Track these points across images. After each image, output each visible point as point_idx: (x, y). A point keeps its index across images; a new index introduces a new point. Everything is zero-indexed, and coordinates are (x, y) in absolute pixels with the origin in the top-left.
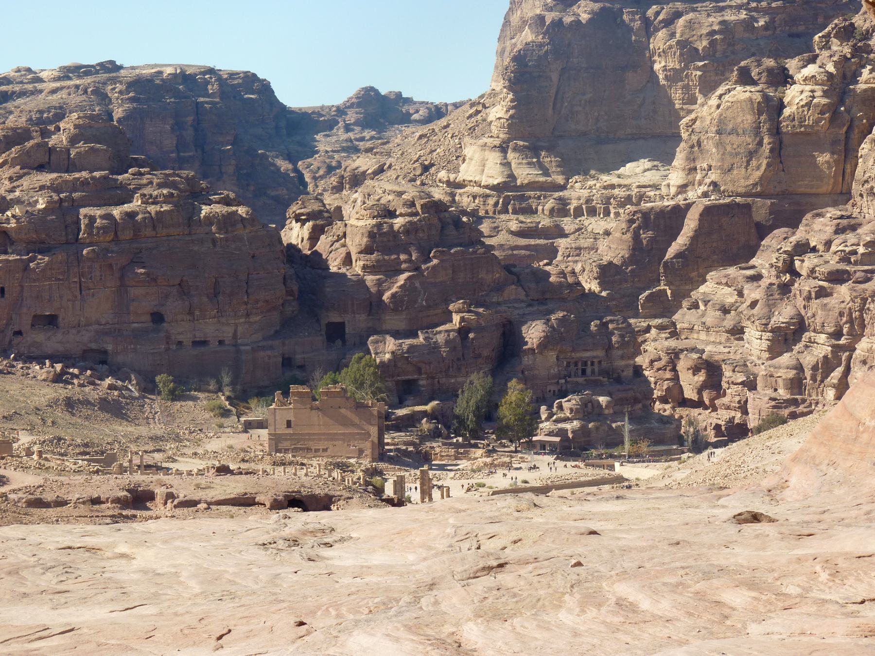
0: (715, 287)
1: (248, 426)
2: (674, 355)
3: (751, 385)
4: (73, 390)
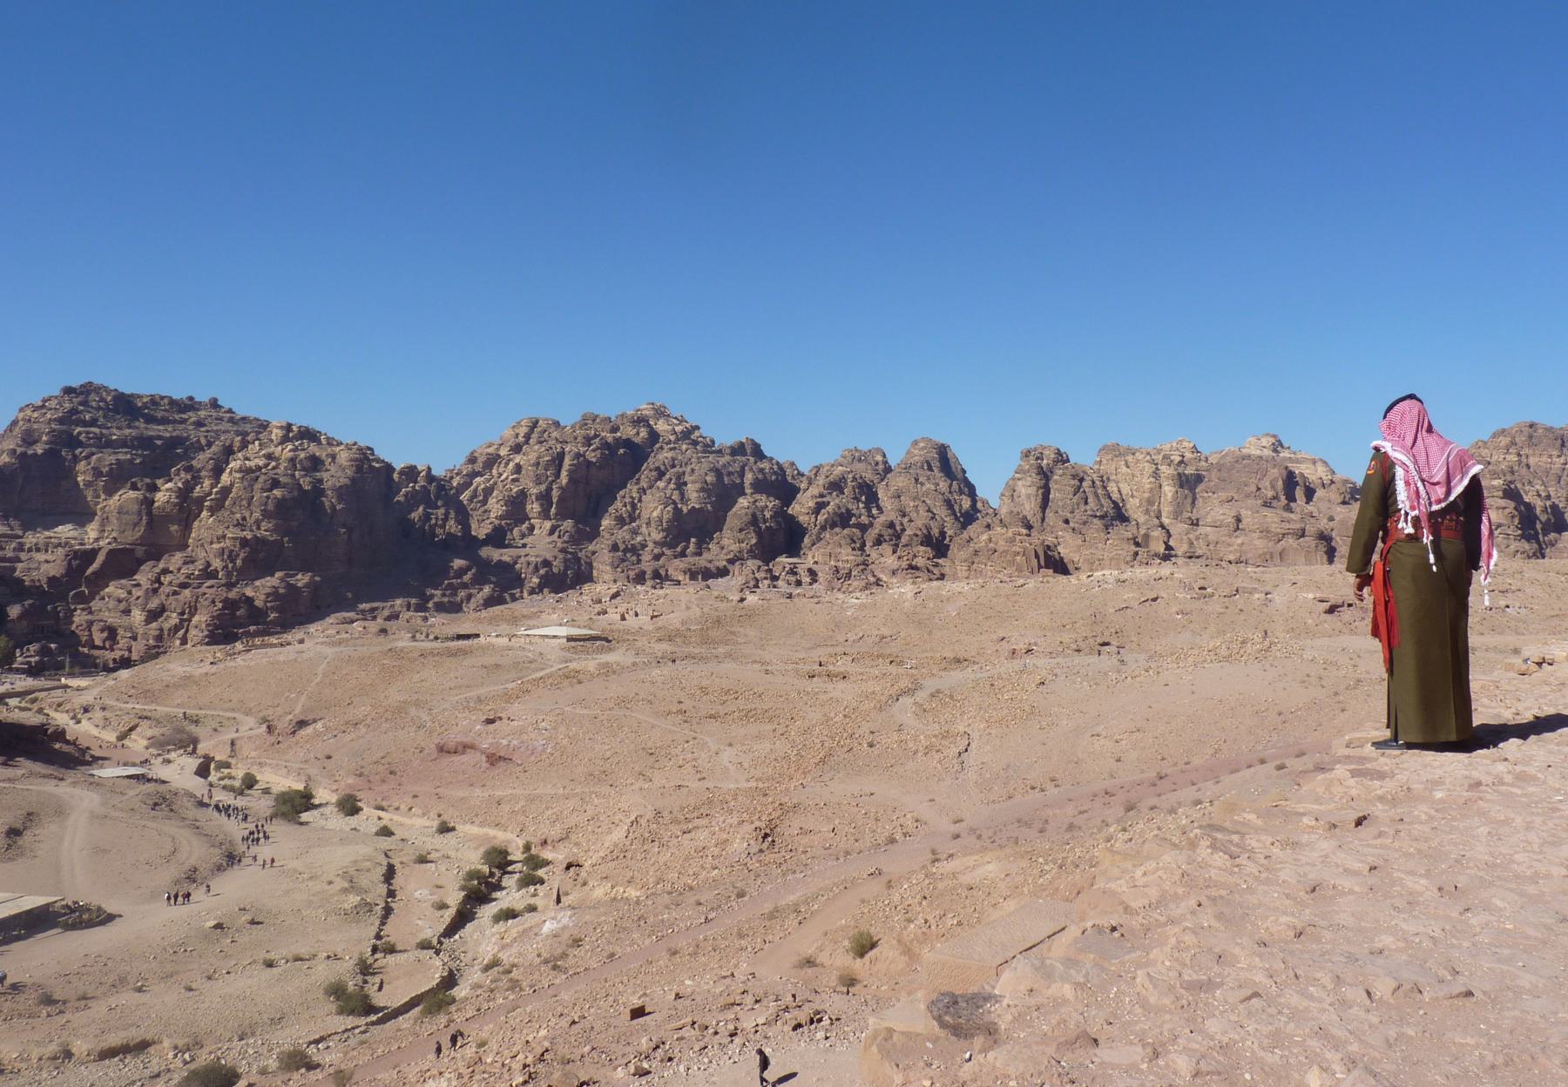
0: (114, 589)
2: (90, 624)
3: (134, 638)
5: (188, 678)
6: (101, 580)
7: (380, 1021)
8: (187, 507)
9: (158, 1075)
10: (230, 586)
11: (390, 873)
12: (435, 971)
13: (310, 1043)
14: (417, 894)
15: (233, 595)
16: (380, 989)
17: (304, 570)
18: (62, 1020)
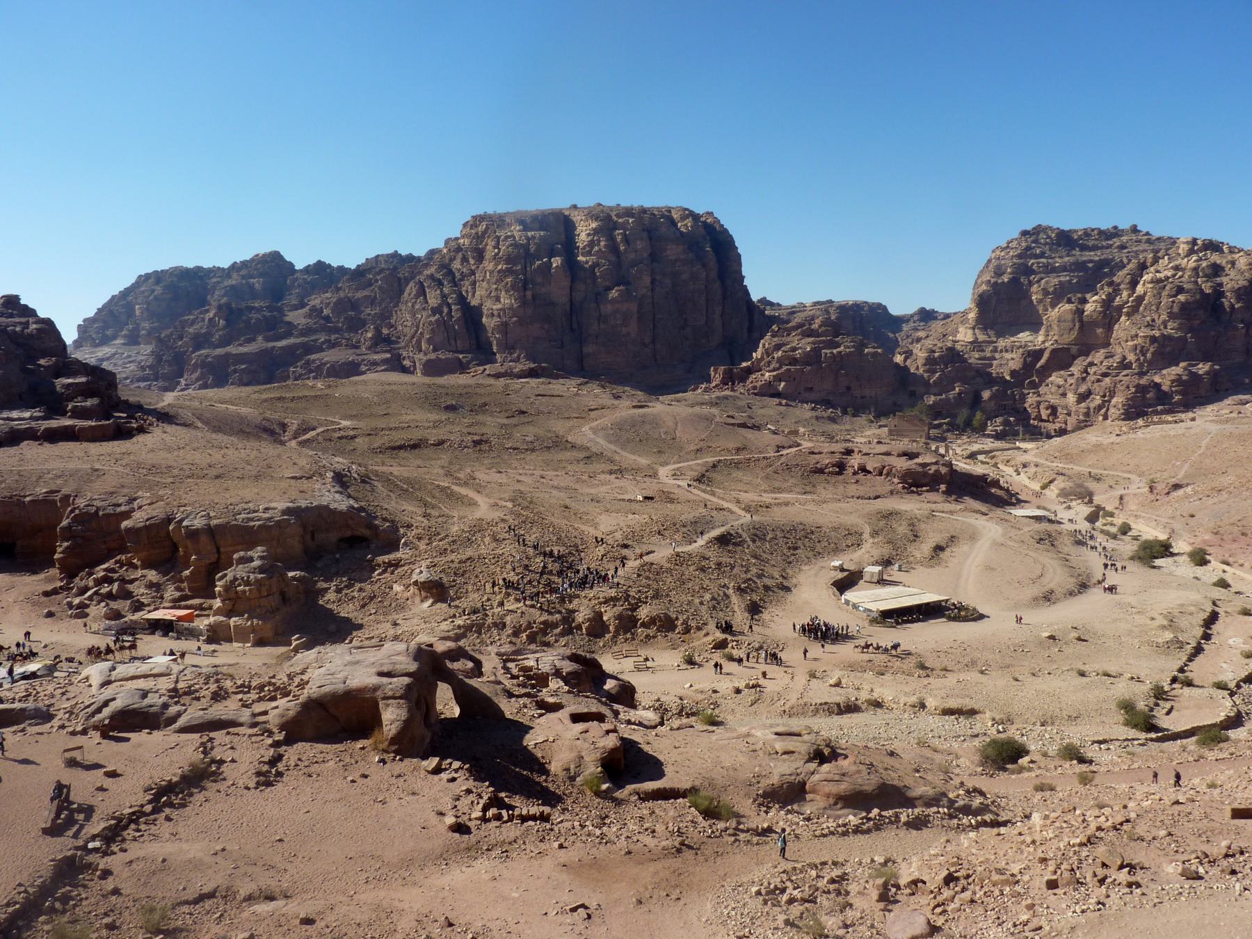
0: (1056, 378)
1: (880, 426)
2: (1039, 403)
3: (1069, 414)
4: (818, 413)
5: (1098, 447)
6: (1045, 372)
7: (1158, 740)
8: (1110, 314)
9: (977, 736)
10: (1141, 374)
11: (1213, 618)
12: (1223, 708)
13: (1094, 742)
14: (1231, 642)
15: (1143, 381)
16: (1168, 713)
17: (1205, 359)
18: (926, 681)
